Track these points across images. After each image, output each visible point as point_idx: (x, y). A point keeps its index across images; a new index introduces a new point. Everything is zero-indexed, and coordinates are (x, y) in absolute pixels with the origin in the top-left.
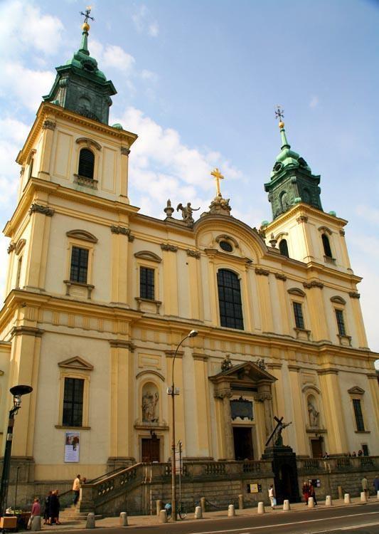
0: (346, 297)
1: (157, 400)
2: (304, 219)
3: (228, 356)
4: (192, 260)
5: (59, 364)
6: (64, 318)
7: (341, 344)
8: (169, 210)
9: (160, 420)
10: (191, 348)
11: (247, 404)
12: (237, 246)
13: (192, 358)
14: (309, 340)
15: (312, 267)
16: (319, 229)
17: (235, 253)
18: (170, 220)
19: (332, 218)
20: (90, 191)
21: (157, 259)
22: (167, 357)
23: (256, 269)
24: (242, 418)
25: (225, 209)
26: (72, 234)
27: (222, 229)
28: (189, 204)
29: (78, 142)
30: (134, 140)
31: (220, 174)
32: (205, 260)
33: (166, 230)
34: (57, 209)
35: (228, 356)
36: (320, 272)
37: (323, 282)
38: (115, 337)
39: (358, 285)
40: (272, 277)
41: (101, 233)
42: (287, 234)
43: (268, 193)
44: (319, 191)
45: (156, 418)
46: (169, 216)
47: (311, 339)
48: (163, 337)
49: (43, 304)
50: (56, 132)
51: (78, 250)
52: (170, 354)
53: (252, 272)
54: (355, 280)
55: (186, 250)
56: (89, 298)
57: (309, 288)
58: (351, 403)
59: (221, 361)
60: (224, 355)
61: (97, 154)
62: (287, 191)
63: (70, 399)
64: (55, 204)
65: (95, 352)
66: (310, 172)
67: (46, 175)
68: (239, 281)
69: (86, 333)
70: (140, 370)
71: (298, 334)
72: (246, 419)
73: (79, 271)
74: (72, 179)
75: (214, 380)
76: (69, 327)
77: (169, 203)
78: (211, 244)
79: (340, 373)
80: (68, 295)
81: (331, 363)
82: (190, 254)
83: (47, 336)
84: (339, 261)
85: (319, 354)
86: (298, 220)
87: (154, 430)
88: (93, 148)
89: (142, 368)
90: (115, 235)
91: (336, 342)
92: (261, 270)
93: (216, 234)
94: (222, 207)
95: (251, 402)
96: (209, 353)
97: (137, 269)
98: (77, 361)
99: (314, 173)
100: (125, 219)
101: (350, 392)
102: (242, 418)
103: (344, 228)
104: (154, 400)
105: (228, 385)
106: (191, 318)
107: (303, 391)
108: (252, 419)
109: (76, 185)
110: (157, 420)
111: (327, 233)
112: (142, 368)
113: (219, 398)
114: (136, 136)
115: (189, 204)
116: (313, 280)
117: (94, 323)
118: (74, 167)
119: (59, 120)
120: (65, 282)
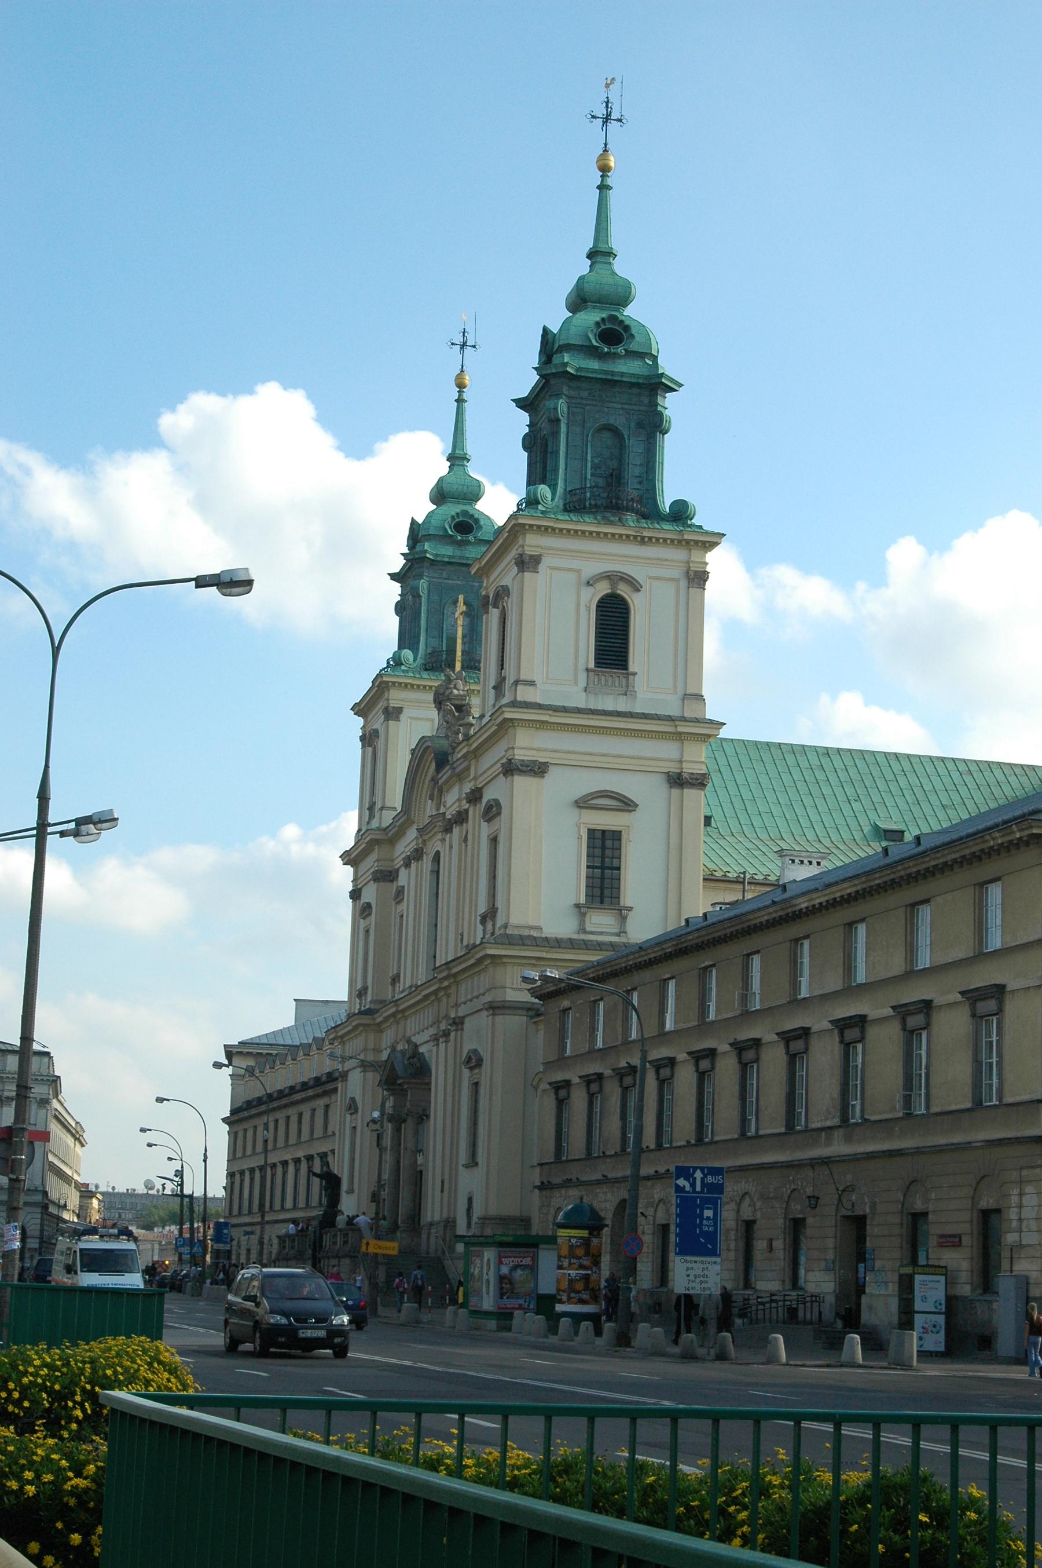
20: (622, 705)
30: (716, 544)
41: (648, 791)
50: (541, 567)
51: (599, 835)
61: (637, 603)
73: (603, 873)
74: (582, 677)
80: (583, 930)
88: (623, 590)
90: (676, 792)
118: (588, 655)
120: (578, 906)
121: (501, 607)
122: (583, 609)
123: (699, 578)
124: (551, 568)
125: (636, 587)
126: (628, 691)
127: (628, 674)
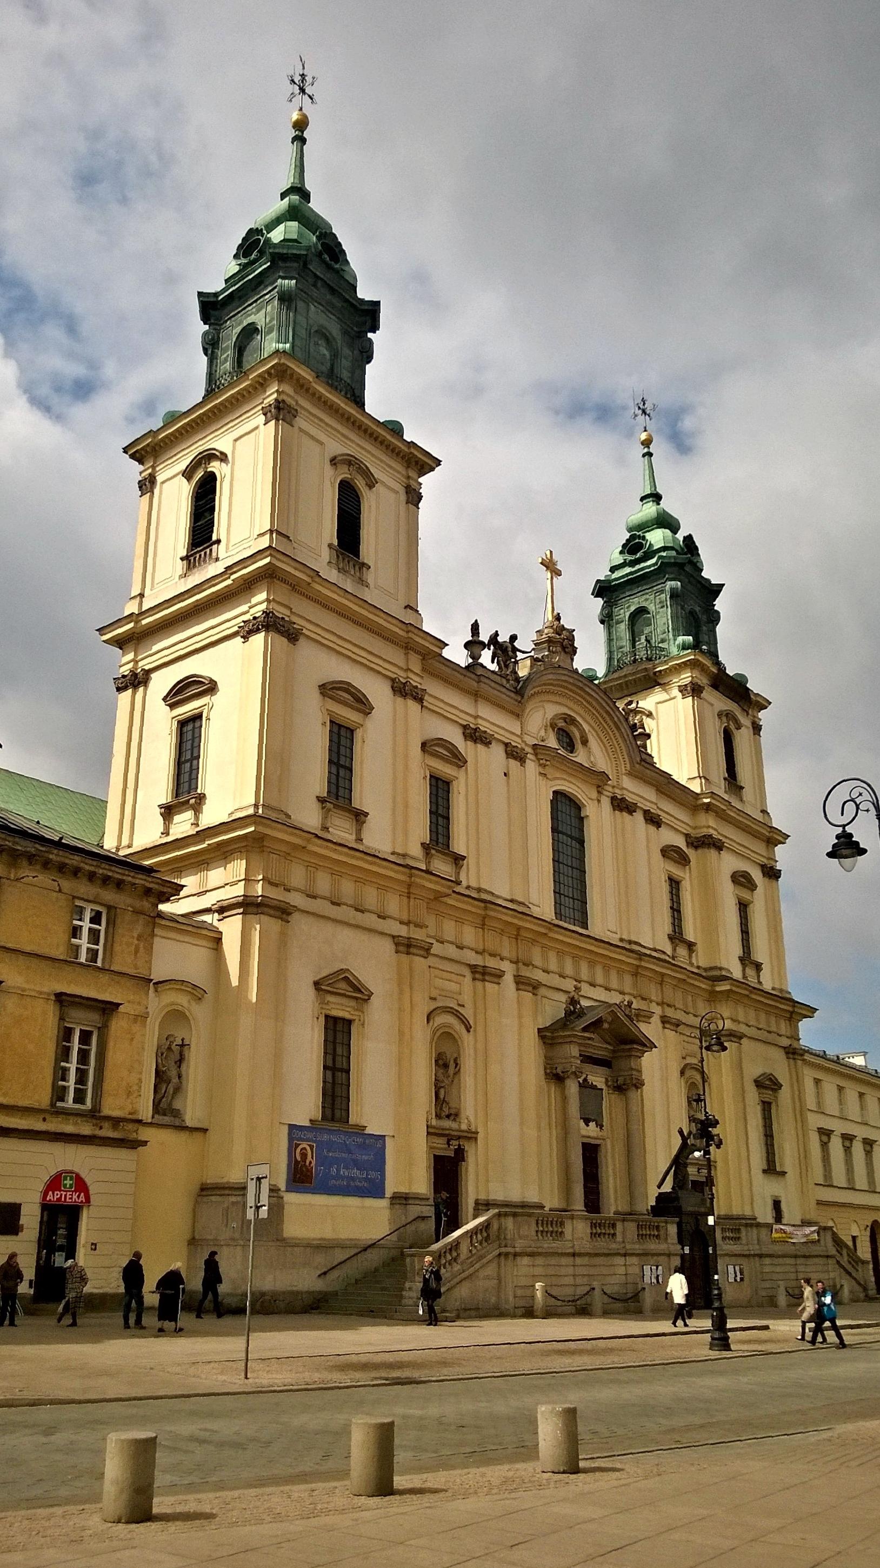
0: (757, 875)
1: (457, 1073)
2: (694, 690)
3: (577, 989)
4: (513, 764)
5: (317, 984)
6: (323, 884)
7: (745, 977)
8: (473, 646)
9: (463, 1115)
10: (511, 962)
11: (594, 1092)
12: (585, 742)
13: (512, 986)
14: (691, 964)
15: (708, 804)
16: (720, 715)
17: (580, 756)
18: (480, 671)
19: (736, 689)
21: (458, 760)
22: (474, 979)
23: (613, 799)
24: (587, 1122)
25: (565, 652)
26: (329, 690)
27: (557, 699)
28: (513, 638)
29: (334, 461)
30: (432, 469)
31: (555, 564)
32: (531, 766)
33: (476, 695)
34: (308, 630)
35: (577, 989)
36: (722, 815)
37: (724, 840)
38: (403, 931)
39: (779, 849)
40: (639, 816)
41: (377, 691)
42: (650, 715)
43: (600, 601)
44: (714, 618)
45: (452, 1111)
46: (475, 657)
47: (694, 961)
48: (469, 935)
49: (295, 847)
52: (481, 974)
53: (606, 802)
54: (774, 838)
55: (506, 745)
56: (359, 840)
57: (696, 848)
58: (759, 1108)
59: (563, 998)
60: (569, 985)
62: (651, 608)
63: (330, 1063)
64: (304, 613)
65: (372, 962)
66: (702, 570)
67: (285, 540)
68: (581, 819)
69: (359, 918)
70: (433, 1005)
71: (674, 950)
72: (592, 1124)
74: (326, 554)
75: (549, 1037)
76: (333, 903)
77: (475, 628)
78: (542, 733)
79: (744, 1041)
80: (325, 828)
81: (734, 1020)
82: (514, 753)
83: (296, 917)
84: (748, 793)
85: (713, 997)
86: (682, 689)
87: (459, 1138)
89: (435, 999)
90: (400, 700)
91: (737, 973)
92: (623, 800)
93: (552, 710)
94: (564, 648)
95: (602, 1089)
96: (539, 976)
97: (425, 778)
98: (346, 979)
99: (710, 573)
100: (415, 664)
101: (758, 1084)
102: (587, 1122)
103: (762, 714)
104: (451, 1070)
105: (574, 1051)
106: (509, 898)
107: (682, 1073)
108: (601, 1127)
109: (335, 572)
110: (457, 1115)
111: (732, 727)
112: (435, 999)
113: (556, 1077)
114: (438, 462)
115: (513, 638)
116: (705, 831)
117: (371, 897)
118: (329, 530)
119: (303, 402)
120: (321, 800)
121: (199, 474)
122: (327, 484)
123: (414, 497)
124: (301, 430)
125: (371, 483)
126: (362, 582)
127: (363, 564)
